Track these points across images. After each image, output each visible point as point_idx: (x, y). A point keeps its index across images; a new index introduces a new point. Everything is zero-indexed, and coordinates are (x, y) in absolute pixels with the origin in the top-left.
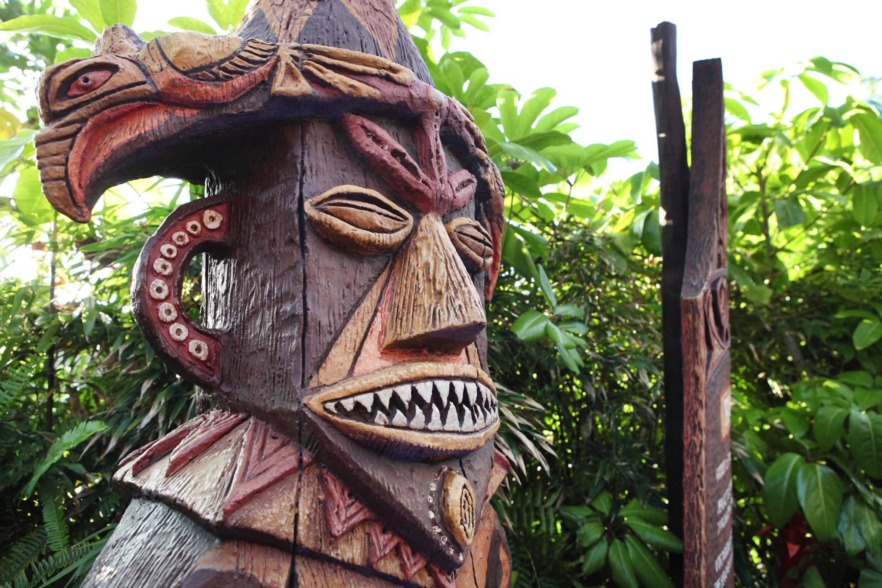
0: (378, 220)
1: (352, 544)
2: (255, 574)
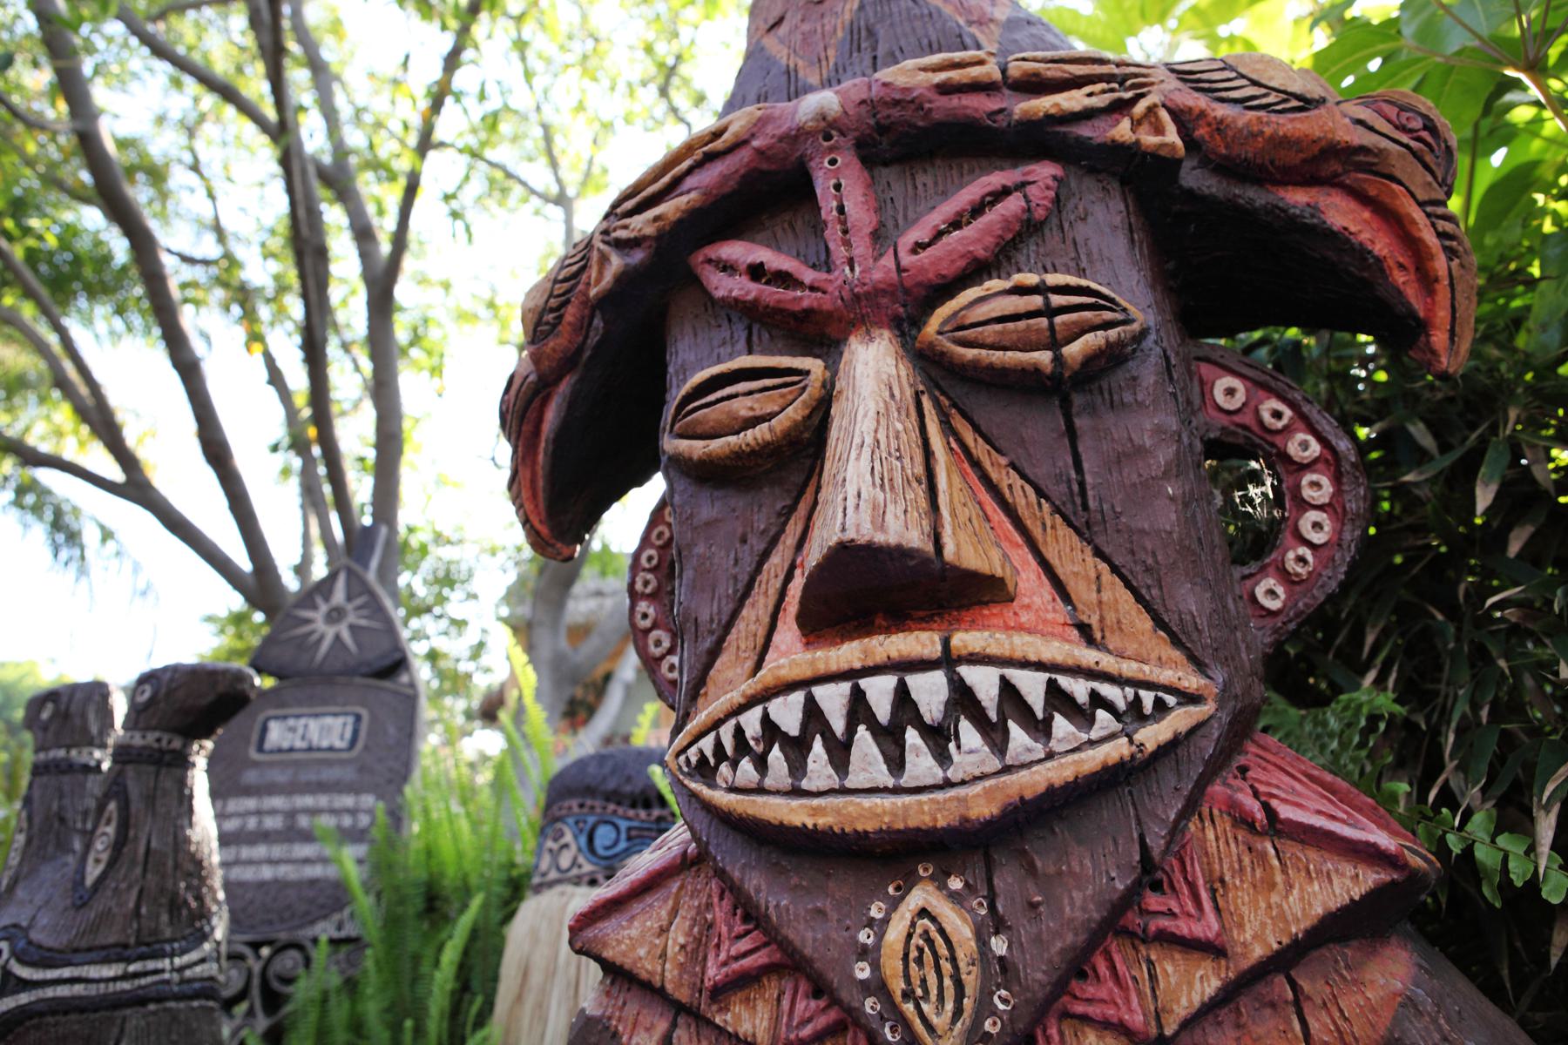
0: (742, 407)
1: (754, 1007)
2: (620, 1028)
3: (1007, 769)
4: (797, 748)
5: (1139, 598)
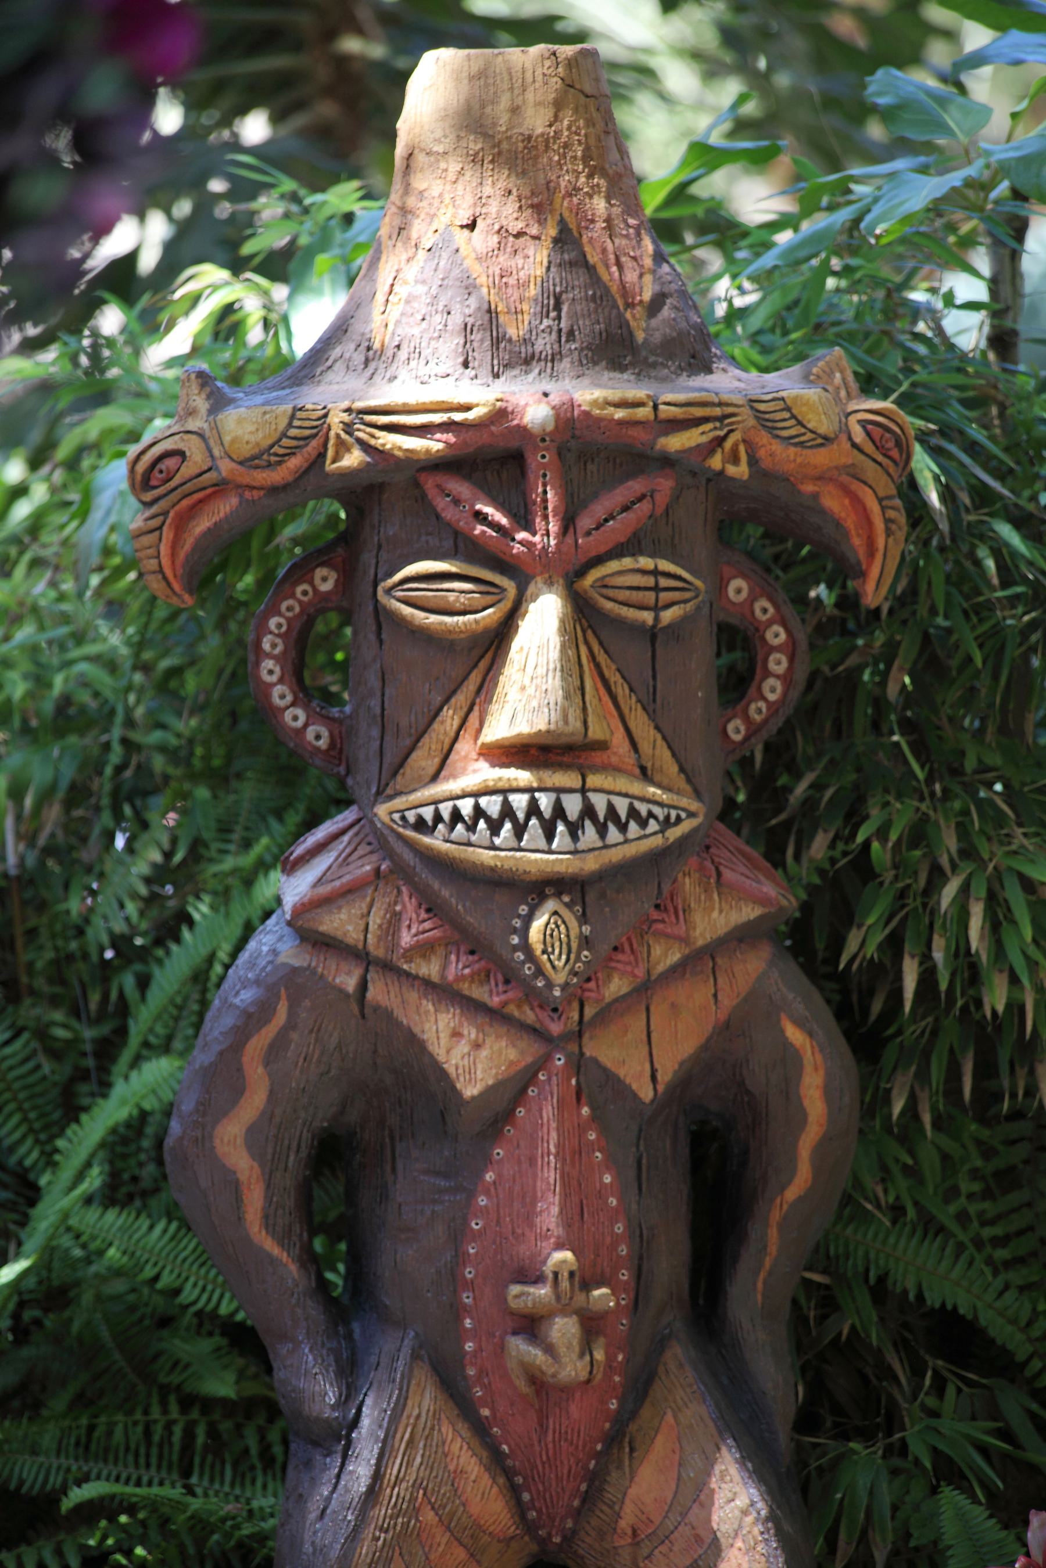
3: (606, 847)
4: (495, 827)
5: (674, 755)
